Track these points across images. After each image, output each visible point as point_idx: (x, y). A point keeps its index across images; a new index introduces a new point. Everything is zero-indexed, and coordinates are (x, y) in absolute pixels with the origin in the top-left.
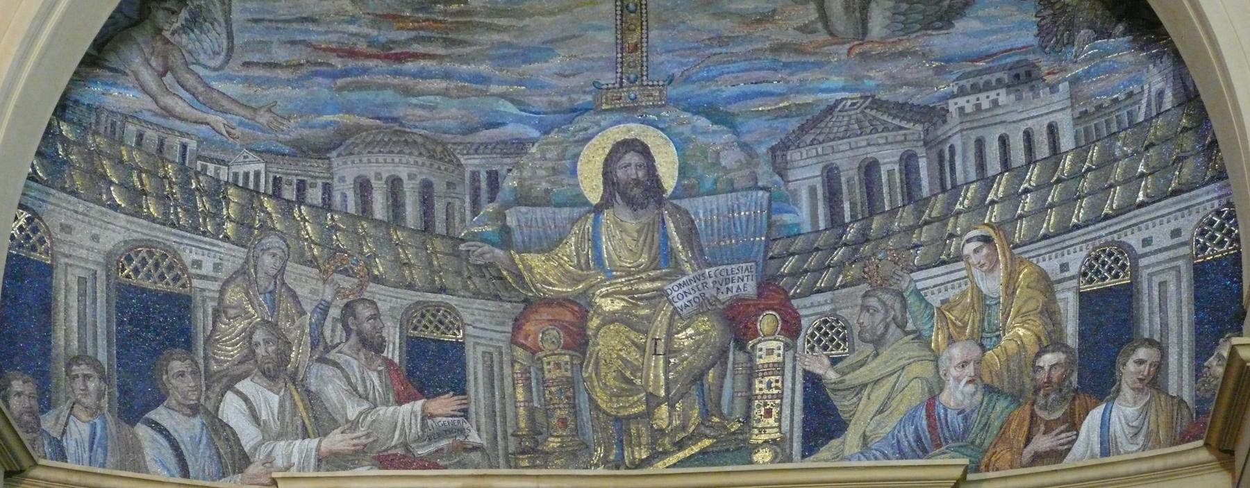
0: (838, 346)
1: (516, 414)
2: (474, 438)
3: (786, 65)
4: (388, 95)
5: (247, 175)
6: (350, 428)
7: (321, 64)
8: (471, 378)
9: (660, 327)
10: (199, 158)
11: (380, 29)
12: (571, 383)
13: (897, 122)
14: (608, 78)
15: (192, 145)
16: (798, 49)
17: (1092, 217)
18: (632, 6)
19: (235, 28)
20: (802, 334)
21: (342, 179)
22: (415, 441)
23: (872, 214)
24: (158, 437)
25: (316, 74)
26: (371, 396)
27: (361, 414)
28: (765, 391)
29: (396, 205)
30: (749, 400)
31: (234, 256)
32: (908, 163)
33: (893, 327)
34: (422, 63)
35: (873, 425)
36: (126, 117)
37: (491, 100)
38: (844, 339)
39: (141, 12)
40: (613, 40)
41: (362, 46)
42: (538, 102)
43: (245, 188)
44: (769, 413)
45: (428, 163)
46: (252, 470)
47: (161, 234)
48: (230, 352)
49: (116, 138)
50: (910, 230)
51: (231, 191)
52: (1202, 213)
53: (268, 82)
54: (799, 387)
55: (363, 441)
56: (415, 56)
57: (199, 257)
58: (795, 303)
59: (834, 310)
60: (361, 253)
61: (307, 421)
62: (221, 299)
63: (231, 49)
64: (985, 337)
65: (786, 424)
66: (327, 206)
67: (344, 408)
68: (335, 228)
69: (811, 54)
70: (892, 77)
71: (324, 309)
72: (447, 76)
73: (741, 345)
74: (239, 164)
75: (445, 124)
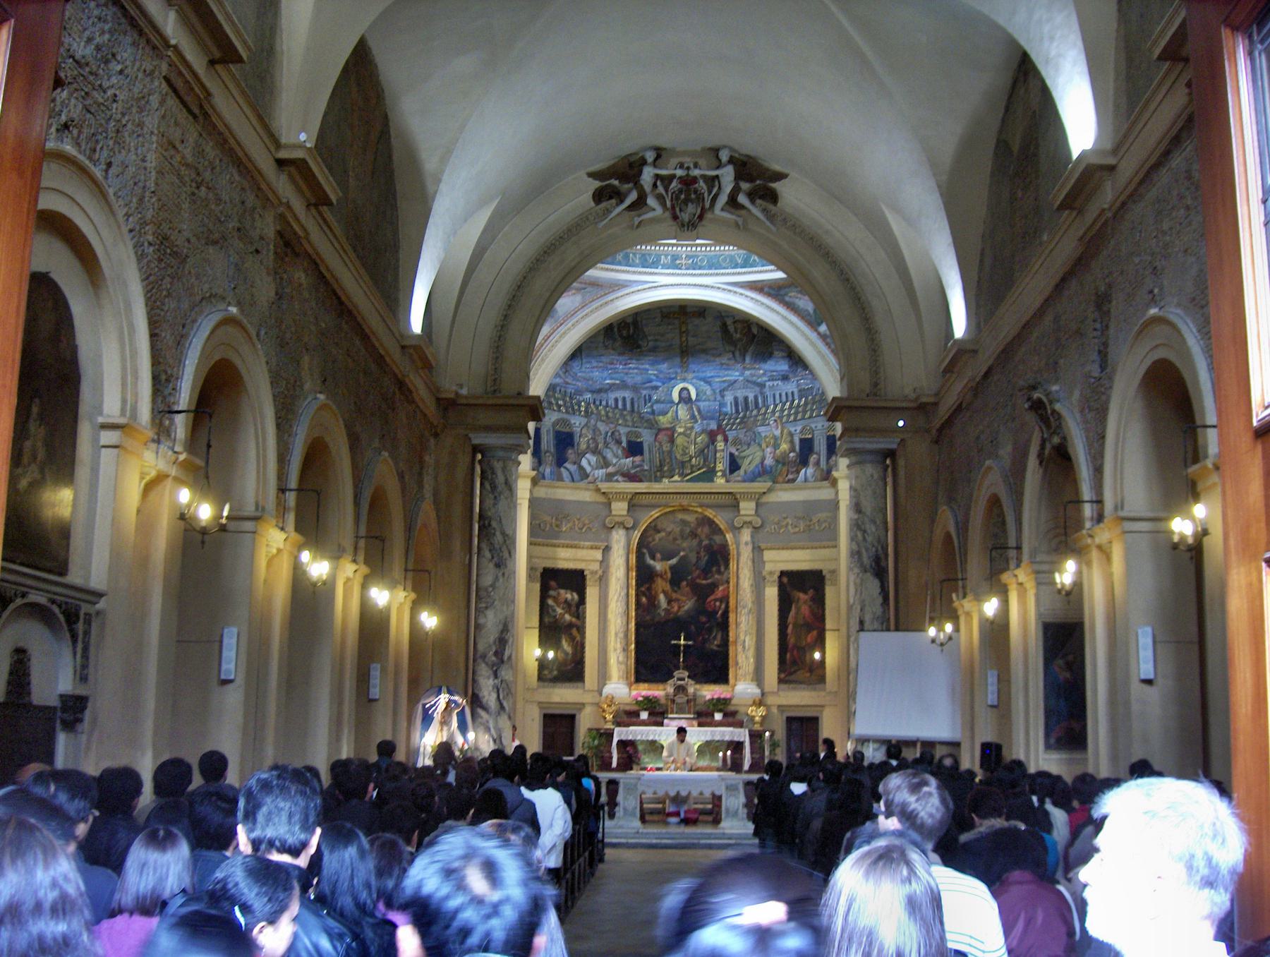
2: (646, 468)
14: (679, 371)
29: (624, 405)
31: (584, 421)
32: (756, 398)
42: (661, 376)
47: (566, 416)
48: (583, 446)
64: (776, 446)
66: (607, 406)
71: (607, 433)
73: (713, 444)
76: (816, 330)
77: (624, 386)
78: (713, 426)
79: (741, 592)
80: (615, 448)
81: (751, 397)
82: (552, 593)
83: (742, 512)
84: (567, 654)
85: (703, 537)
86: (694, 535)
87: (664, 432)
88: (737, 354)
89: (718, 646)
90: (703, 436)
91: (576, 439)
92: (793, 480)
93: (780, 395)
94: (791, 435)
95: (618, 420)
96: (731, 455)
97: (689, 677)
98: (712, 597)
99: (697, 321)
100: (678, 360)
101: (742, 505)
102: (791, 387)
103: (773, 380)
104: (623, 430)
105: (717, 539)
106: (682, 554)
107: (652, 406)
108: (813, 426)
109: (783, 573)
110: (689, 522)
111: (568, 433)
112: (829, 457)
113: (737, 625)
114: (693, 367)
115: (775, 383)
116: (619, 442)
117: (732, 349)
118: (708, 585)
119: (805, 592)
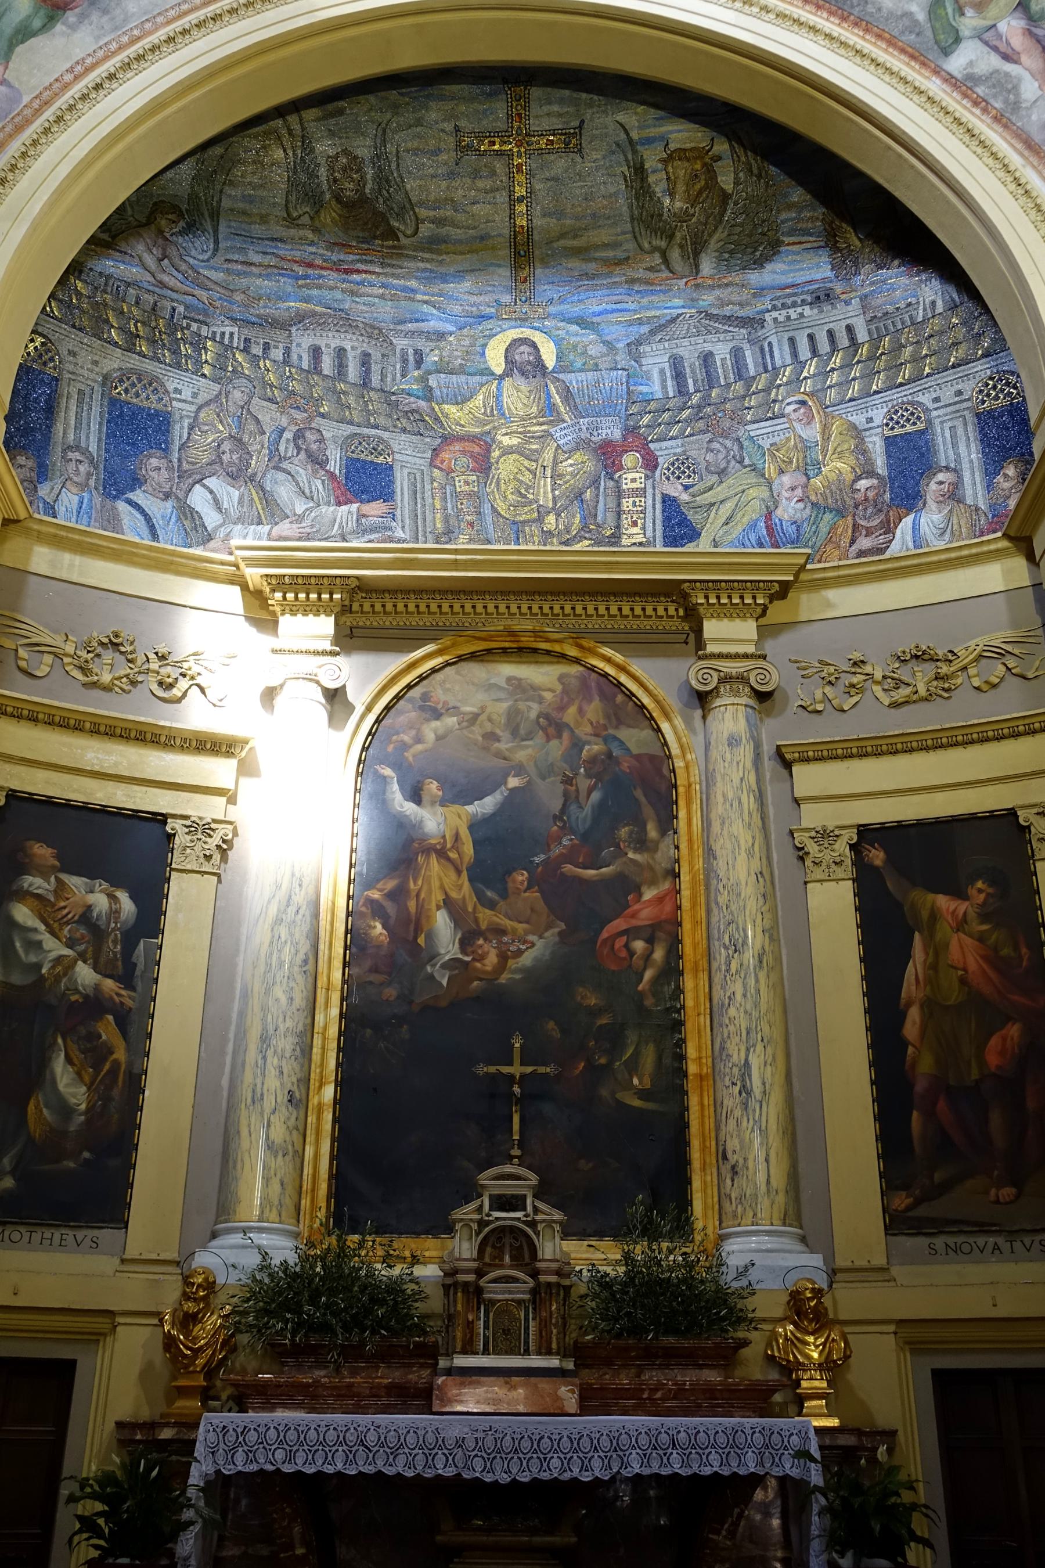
0: (689, 477)
1: (434, 518)
2: (399, 533)
3: (637, 292)
5: (223, 334)
6: (296, 521)
7: (286, 269)
8: (398, 491)
9: (548, 456)
10: (185, 317)
11: (333, 252)
13: (726, 327)
14: (506, 298)
15: (181, 309)
16: (648, 282)
17: (888, 384)
18: (522, 253)
19: (220, 236)
20: (659, 468)
21: (299, 345)
22: (350, 534)
23: (711, 388)
24: (134, 511)
25: (283, 275)
26: (315, 498)
27: (307, 509)
28: (631, 508)
30: (619, 514)
31: (208, 389)
32: (737, 354)
33: (733, 463)
34: (364, 276)
35: (721, 532)
36: (128, 284)
37: (416, 304)
38: (694, 473)
39: (148, 218)
40: (509, 274)
41: (319, 262)
43: (221, 343)
44: (635, 524)
45: (367, 341)
47: (149, 366)
50: (744, 397)
51: (209, 343)
52: (978, 379)
55: (308, 530)
56: (358, 271)
57: (179, 387)
58: (650, 445)
59: (685, 452)
60: (312, 397)
61: (261, 512)
62: (196, 418)
63: (216, 250)
64: (809, 468)
65: (649, 533)
66: (287, 361)
67: (293, 505)
69: (656, 285)
70: (719, 299)
71: (282, 431)
72: (384, 286)
74: (218, 325)
75: (380, 317)
76: (937, 71)
78: (612, 430)
79: (723, 899)
80: (302, 474)
81: (721, 351)
82: (34, 883)
83: (710, 648)
84: (66, 1111)
85: (584, 731)
87: (457, 447)
88: (675, 254)
89: (644, 1094)
91: (179, 431)
92: (881, 551)
93: (811, 337)
94: (857, 433)
96: (667, 501)
97: (539, 1194)
98: (619, 924)
99: (560, 164)
100: (506, 272)
101: (711, 628)
103: (784, 306)
104: (331, 431)
106: (513, 782)
107: (423, 379)
108: (925, 399)
110: (534, 688)
112: (992, 468)
114: (546, 290)
116: (317, 461)
117: (663, 244)
118: (605, 883)
119: (960, 894)
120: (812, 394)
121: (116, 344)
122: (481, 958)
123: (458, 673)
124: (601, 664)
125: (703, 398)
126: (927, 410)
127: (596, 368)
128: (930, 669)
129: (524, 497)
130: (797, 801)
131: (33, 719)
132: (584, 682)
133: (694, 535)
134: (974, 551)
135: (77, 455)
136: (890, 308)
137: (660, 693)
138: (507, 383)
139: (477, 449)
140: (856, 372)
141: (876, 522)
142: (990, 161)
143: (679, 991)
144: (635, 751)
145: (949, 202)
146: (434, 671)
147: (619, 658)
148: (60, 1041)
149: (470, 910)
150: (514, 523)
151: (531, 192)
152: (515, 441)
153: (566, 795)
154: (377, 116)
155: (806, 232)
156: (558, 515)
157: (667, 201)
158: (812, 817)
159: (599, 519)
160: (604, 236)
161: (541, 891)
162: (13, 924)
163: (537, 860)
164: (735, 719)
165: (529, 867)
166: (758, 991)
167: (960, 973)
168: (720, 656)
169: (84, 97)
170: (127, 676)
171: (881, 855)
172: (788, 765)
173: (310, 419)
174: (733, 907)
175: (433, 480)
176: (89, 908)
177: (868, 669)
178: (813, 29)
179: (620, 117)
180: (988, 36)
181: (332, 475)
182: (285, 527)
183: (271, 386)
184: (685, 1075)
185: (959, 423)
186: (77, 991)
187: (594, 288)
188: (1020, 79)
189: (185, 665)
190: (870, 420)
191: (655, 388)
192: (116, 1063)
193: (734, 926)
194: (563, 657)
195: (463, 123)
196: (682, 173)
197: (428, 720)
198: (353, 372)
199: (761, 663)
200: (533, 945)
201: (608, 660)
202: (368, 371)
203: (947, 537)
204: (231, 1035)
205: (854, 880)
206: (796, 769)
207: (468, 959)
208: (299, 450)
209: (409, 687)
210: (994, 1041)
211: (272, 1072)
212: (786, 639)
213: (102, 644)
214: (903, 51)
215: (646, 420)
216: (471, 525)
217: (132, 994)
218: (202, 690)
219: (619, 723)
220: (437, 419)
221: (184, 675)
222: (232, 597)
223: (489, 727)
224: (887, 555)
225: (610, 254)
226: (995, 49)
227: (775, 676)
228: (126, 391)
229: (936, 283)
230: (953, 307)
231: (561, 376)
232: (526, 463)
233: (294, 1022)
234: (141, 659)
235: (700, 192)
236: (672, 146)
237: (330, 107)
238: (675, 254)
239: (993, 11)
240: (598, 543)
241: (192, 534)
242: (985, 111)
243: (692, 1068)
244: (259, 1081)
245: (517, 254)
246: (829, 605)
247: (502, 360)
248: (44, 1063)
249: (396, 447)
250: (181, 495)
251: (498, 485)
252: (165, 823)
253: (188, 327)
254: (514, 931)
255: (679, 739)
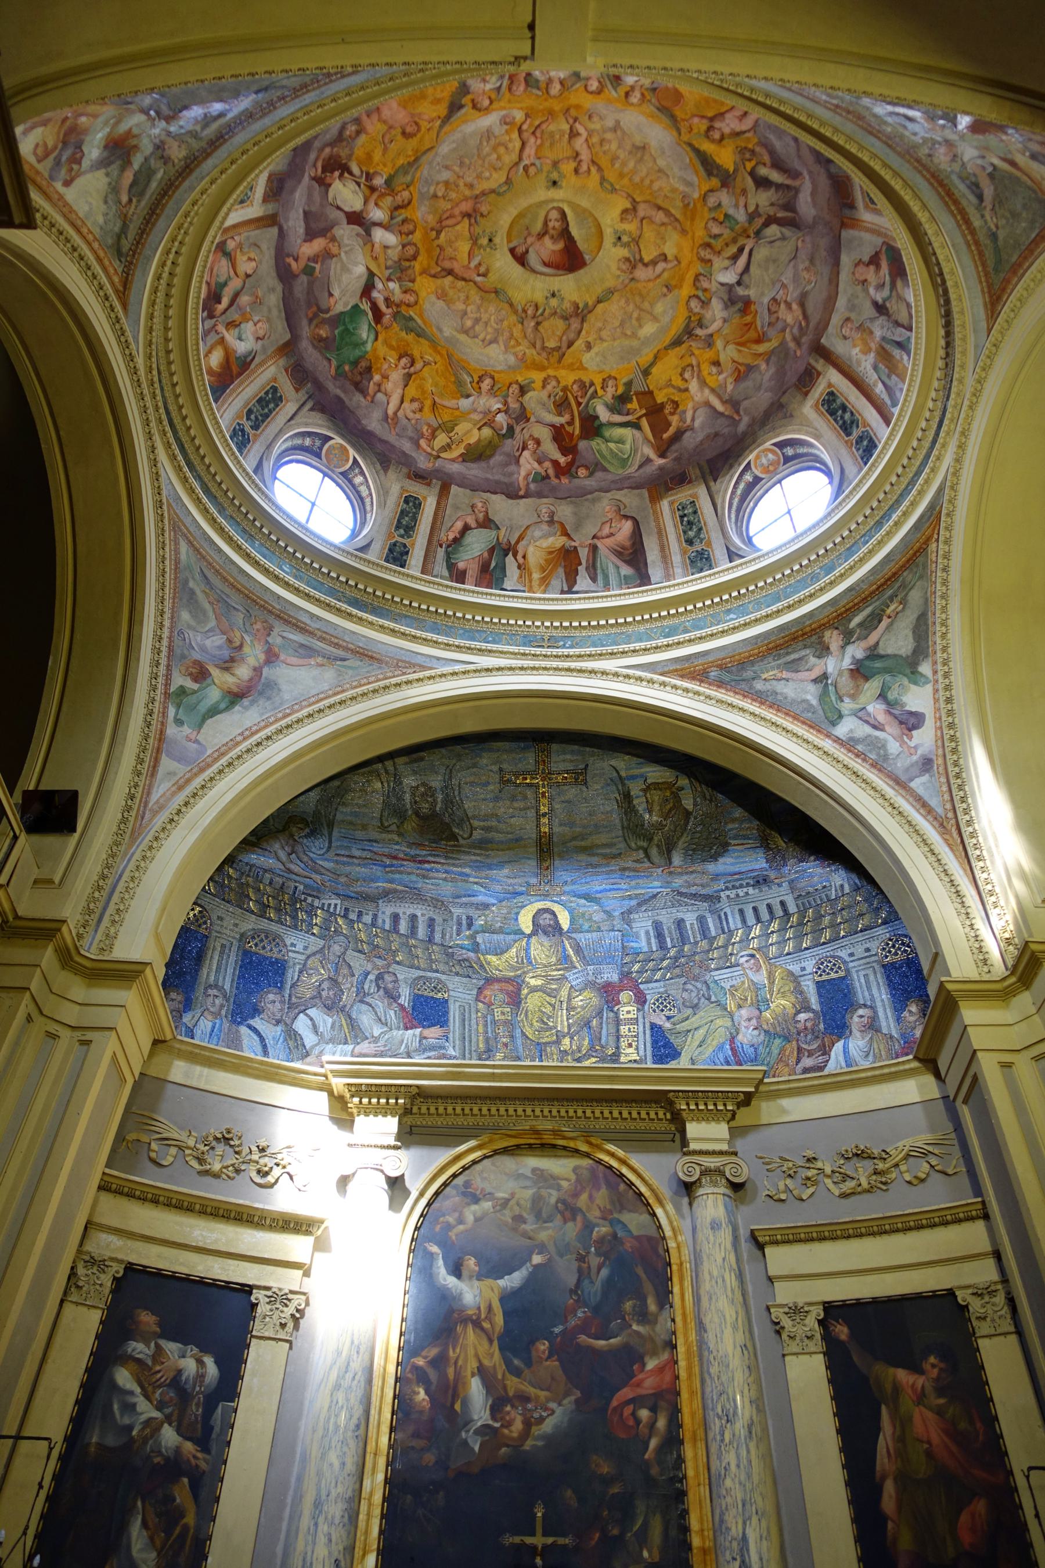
2: (451, 1052)
4: (413, 878)
9: (564, 993)
12: (510, 1025)
14: (534, 881)
15: (301, 887)
16: (635, 870)
23: (684, 944)
30: (618, 1038)
32: (701, 920)
36: (265, 871)
41: (401, 855)
44: (630, 1045)
46: (308, 1059)
47: (274, 927)
49: (258, 879)
50: (708, 951)
53: (349, 864)
54: (648, 1032)
56: (429, 862)
62: (304, 965)
63: (330, 847)
64: (760, 1004)
65: (642, 1053)
68: (376, 936)
71: (367, 974)
72: (446, 872)
76: (828, 735)
77: (417, 896)
78: (611, 975)
79: (714, 1370)
80: (380, 1005)
81: (690, 918)
82: (138, 1348)
83: (693, 1146)
85: (594, 1215)
86: (568, 1210)
87: (496, 986)
88: (654, 852)
90: (586, 994)
91: (292, 974)
92: (821, 1069)
93: (755, 909)
94: (794, 979)
95: (395, 953)
98: (626, 1393)
99: (572, 792)
101: (693, 1129)
102: (780, 894)
103: (734, 887)
104: (404, 974)
105: (635, 1221)
106: (537, 1259)
107: (473, 937)
108: (843, 954)
109: (832, 1311)
110: (553, 1177)
111: (277, 961)
113: (713, 1483)
115: (741, 892)
116: (392, 996)
117: (645, 844)
118: (613, 1352)
119: (916, 1368)
120: (758, 950)
121: (252, 912)
122: (508, 1425)
123: (493, 1164)
124: (606, 1158)
125: (678, 952)
126: (845, 962)
127: (599, 930)
128: (869, 1165)
129: (546, 1024)
130: (770, 1279)
131: (155, 1201)
132: (593, 1172)
133: (676, 1054)
134: (893, 1069)
135: (215, 992)
136: (811, 889)
137: (653, 1182)
138: (534, 940)
139: (511, 988)
140: (790, 934)
141: (815, 1046)
142: (872, 792)
143: (680, 1460)
144: (635, 1233)
145: (845, 819)
146: (475, 1162)
147: (620, 1153)
148: (139, 1503)
149: (500, 1377)
150: (538, 1044)
151: (551, 810)
152: (539, 982)
153: (580, 1271)
154: (446, 761)
155: (745, 837)
156: (572, 1038)
157: (647, 816)
158: (785, 1294)
159: (603, 1042)
160: (603, 838)
161: (559, 1360)
162: (114, 1387)
163: (557, 1330)
164: (716, 1206)
165: (549, 1336)
166: (750, 1462)
167: (926, 1446)
168: (701, 1153)
169: (248, 751)
170: (233, 1165)
171: (845, 1330)
172: (761, 1247)
173: (389, 965)
174: (724, 1378)
175: (477, 1011)
176: (180, 1372)
177: (819, 1165)
178: (742, 710)
179: (613, 762)
180: (861, 714)
181: (402, 1006)
182: (365, 1047)
183: (362, 941)
184: (690, 1548)
185: (870, 972)
186: (159, 1453)
187: (597, 874)
188: (886, 741)
189: (279, 1156)
190: (803, 969)
191: (643, 944)
192: (186, 1528)
193: (724, 1396)
194: (577, 1152)
195: (505, 766)
196: (656, 798)
197: (468, 1204)
198: (422, 932)
199: (733, 1159)
200: (553, 1412)
201: (612, 1155)
202: (433, 931)
203: (871, 1058)
204: (289, 1500)
205: (825, 1354)
206: (768, 1250)
207: (497, 1425)
208: (379, 988)
209: (454, 1176)
210: (964, 1518)
211: (322, 1539)
212: (752, 1138)
213: (216, 1139)
214: (803, 723)
215: (636, 967)
216: (506, 1045)
217: (207, 1457)
218: (291, 1177)
219: (622, 1208)
220: (482, 966)
221: (277, 1165)
222: (320, 1101)
223: (517, 1211)
224: (826, 1072)
225: (608, 851)
226: (867, 722)
227: (745, 1169)
228: (256, 945)
229: (842, 873)
230: (857, 889)
231: (573, 935)
232: (548, 998)
233: (343, 1489)
234: (245, 1151)
235: (670, 811)
236: (649, 781)
237: (414, 756)
238: (654, 852)
239: (862, 699)
240: (602, 1060)
241: (294, 1051)
242: (864, 760)
243: (696, 1541)
244: (309, 1549)
245: (542, 850)
246: (784, 1111)
247: (530, 924)
248: (123, 1527)
249: (451, 986)
250: (288, 1022)
251: (526, 1015)
252: (250, 1293)
253: (305, 900)
254: (537, 1397)
255: (671, 1223)
